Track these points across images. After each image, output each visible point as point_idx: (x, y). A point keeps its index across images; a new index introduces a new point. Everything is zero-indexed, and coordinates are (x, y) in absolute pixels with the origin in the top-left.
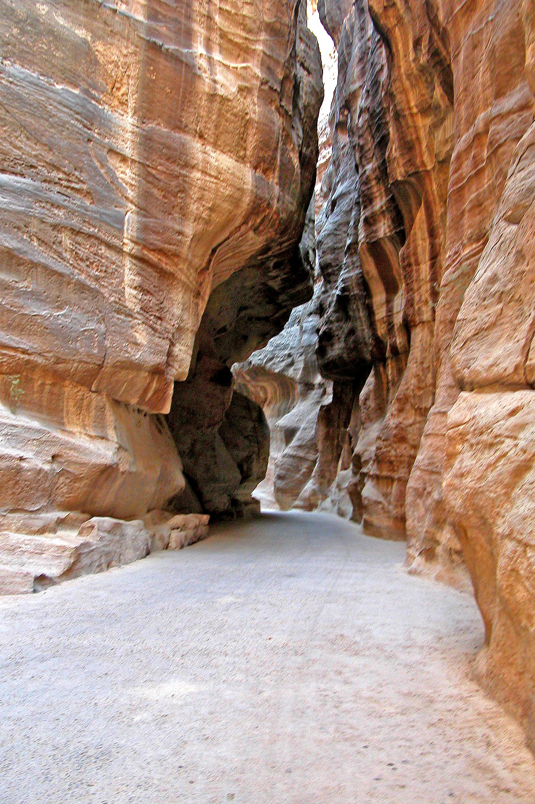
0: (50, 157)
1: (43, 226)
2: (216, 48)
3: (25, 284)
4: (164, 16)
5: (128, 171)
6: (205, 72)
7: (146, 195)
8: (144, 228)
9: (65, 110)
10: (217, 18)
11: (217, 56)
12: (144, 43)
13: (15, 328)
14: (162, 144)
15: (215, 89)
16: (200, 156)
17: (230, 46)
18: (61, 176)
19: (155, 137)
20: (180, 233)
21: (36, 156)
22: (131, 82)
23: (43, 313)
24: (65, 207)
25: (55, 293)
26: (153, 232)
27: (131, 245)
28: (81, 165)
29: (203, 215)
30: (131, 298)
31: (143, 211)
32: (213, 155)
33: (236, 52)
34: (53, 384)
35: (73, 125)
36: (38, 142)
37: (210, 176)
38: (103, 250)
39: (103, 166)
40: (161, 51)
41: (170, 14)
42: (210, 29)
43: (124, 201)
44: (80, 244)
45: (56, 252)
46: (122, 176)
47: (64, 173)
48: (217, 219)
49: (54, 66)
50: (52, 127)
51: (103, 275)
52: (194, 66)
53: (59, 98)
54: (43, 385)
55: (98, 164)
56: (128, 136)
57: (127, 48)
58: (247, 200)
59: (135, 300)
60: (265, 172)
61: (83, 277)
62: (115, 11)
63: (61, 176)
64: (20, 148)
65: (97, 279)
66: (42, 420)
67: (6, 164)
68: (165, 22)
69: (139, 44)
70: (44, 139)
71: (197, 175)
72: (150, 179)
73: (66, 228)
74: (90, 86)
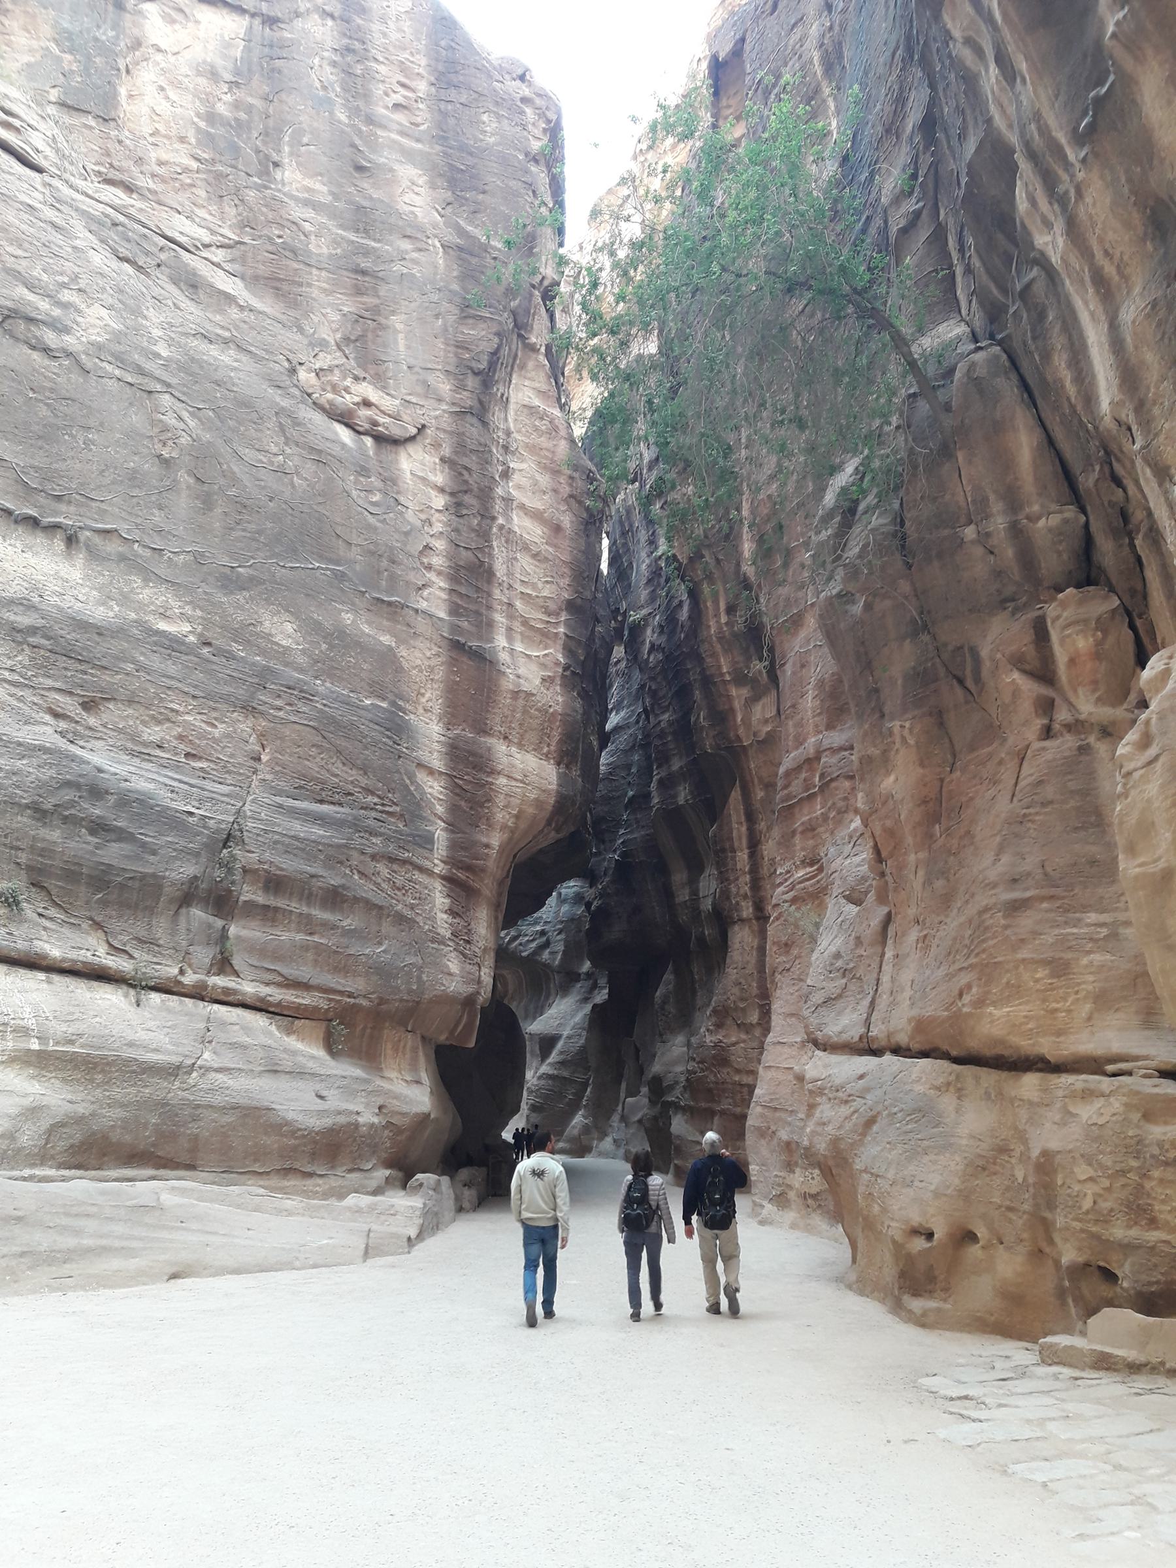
0: (364, 781)
1: (362, 857)
2: (519, 637)
3: (349, 921)
4: (465, 609)
5: (435, 784)
6: (509, 667)
7: (453, 809)
8: (453, 846)
9: (376, 727)
10: (518, 604)
11: (519, 647)
12: (446, 641)
13: (340, 971)
14: (468, 752)
15: (519, 685)
16: (505, 760)
17: (531, 634)
18: (376, 800)
19: (461, 744)
20: (487, 846)
21: (352, 782)
22: (436, 686)
23: (367, 951)
24: (381, 835)
25: (375, 928)
26: (462, 848)
27: (442, 865)
28: (393, 785)
29: (510, 824)
30: (443, 922)
31: (452, 827)
32: (518, 756)
33: (538, 638)
34: (373, 1028)
35: (385, 744)
36: (354, 766)
37: (516, 780)
38: (417, 876)
39: (412, 783)
40: (464, 650)
41: (471, 607)
42: (511, 617)
43: (432, 818)
44: (395, 872)
45: (375, 883)
46: (430, 790)
47: (379, 797)
48: (523, 826)
49: (362, 680)
50: (366, 748)
51: (416, 902)
52: (498, 661)
53: (370, 716)
54: (364, 1029)
55: (408, 781)
56: (436, 746)
57: (430, 649)
58: (552, 801)
59: (446, 926)
60: (567, 767)
61: (400, 907)
62: (417, 611)
63: (376, 800)
64: (336, 776)
65: (412, 907)
66: (363, 1068)
67: (324, 794)
68: (467, 616)
69: (442, 644)
70: (359, 762)
71: (502, 781)
72: (458, 791)
73: (383, 857)
74: (396, 696)
